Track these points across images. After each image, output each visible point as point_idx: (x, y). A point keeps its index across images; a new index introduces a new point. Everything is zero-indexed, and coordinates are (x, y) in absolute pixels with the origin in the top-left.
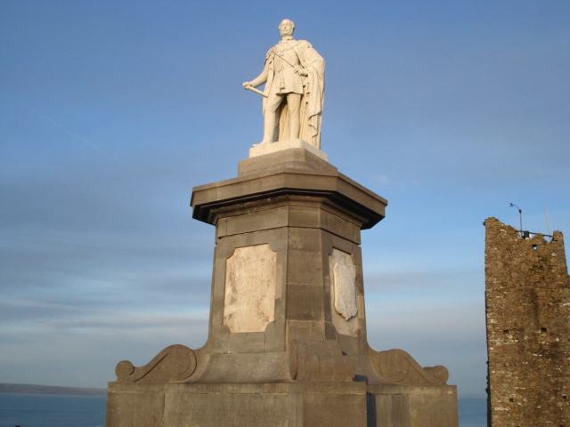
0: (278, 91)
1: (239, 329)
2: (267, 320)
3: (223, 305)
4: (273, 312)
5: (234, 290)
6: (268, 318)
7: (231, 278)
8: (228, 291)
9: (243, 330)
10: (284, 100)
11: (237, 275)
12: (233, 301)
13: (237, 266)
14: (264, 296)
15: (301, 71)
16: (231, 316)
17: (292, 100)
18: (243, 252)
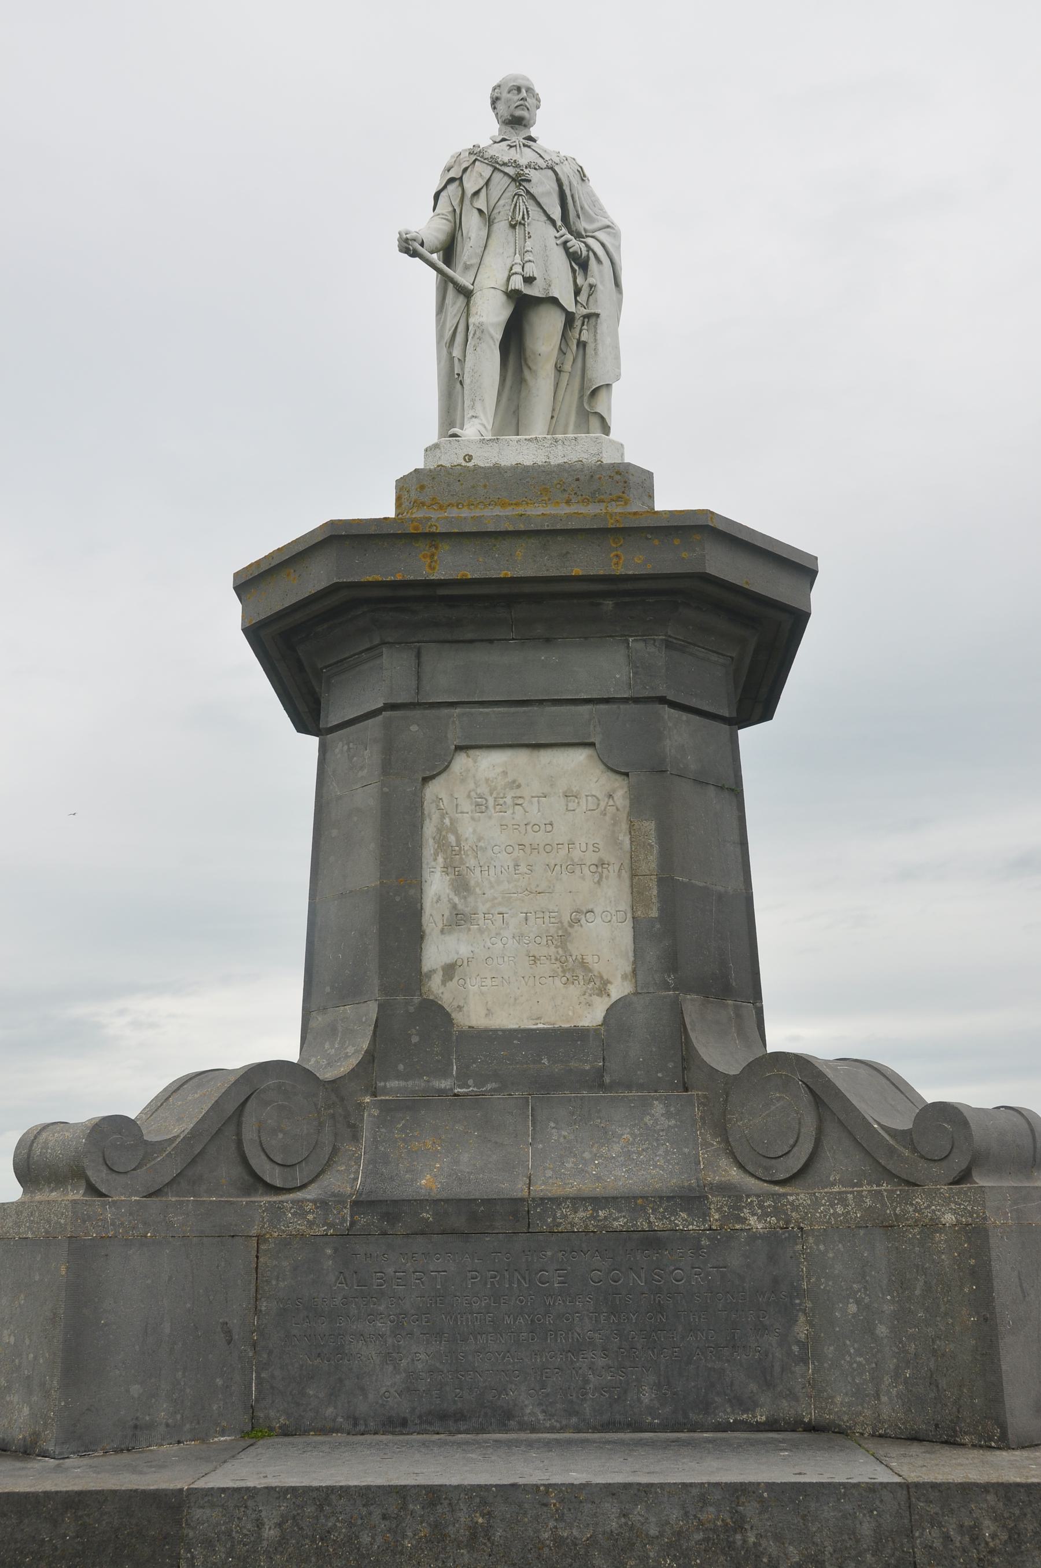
0: (517, 283)
1: (489, 1013)
2: (602, 990)
3: (417, 936)
4: (625, 966)
5: (461, 886)
6: (606, 983)
7: (442, 844)
8: (436, 885)
9: (509, 1019)
10: (522, 306)
11: (467, 830)
12: (458, 920)
13: (466, 806)
14: (579, 915)
15: (575, 245)
16: (450, 970)
17: (545, 333)
18: (489, 765)
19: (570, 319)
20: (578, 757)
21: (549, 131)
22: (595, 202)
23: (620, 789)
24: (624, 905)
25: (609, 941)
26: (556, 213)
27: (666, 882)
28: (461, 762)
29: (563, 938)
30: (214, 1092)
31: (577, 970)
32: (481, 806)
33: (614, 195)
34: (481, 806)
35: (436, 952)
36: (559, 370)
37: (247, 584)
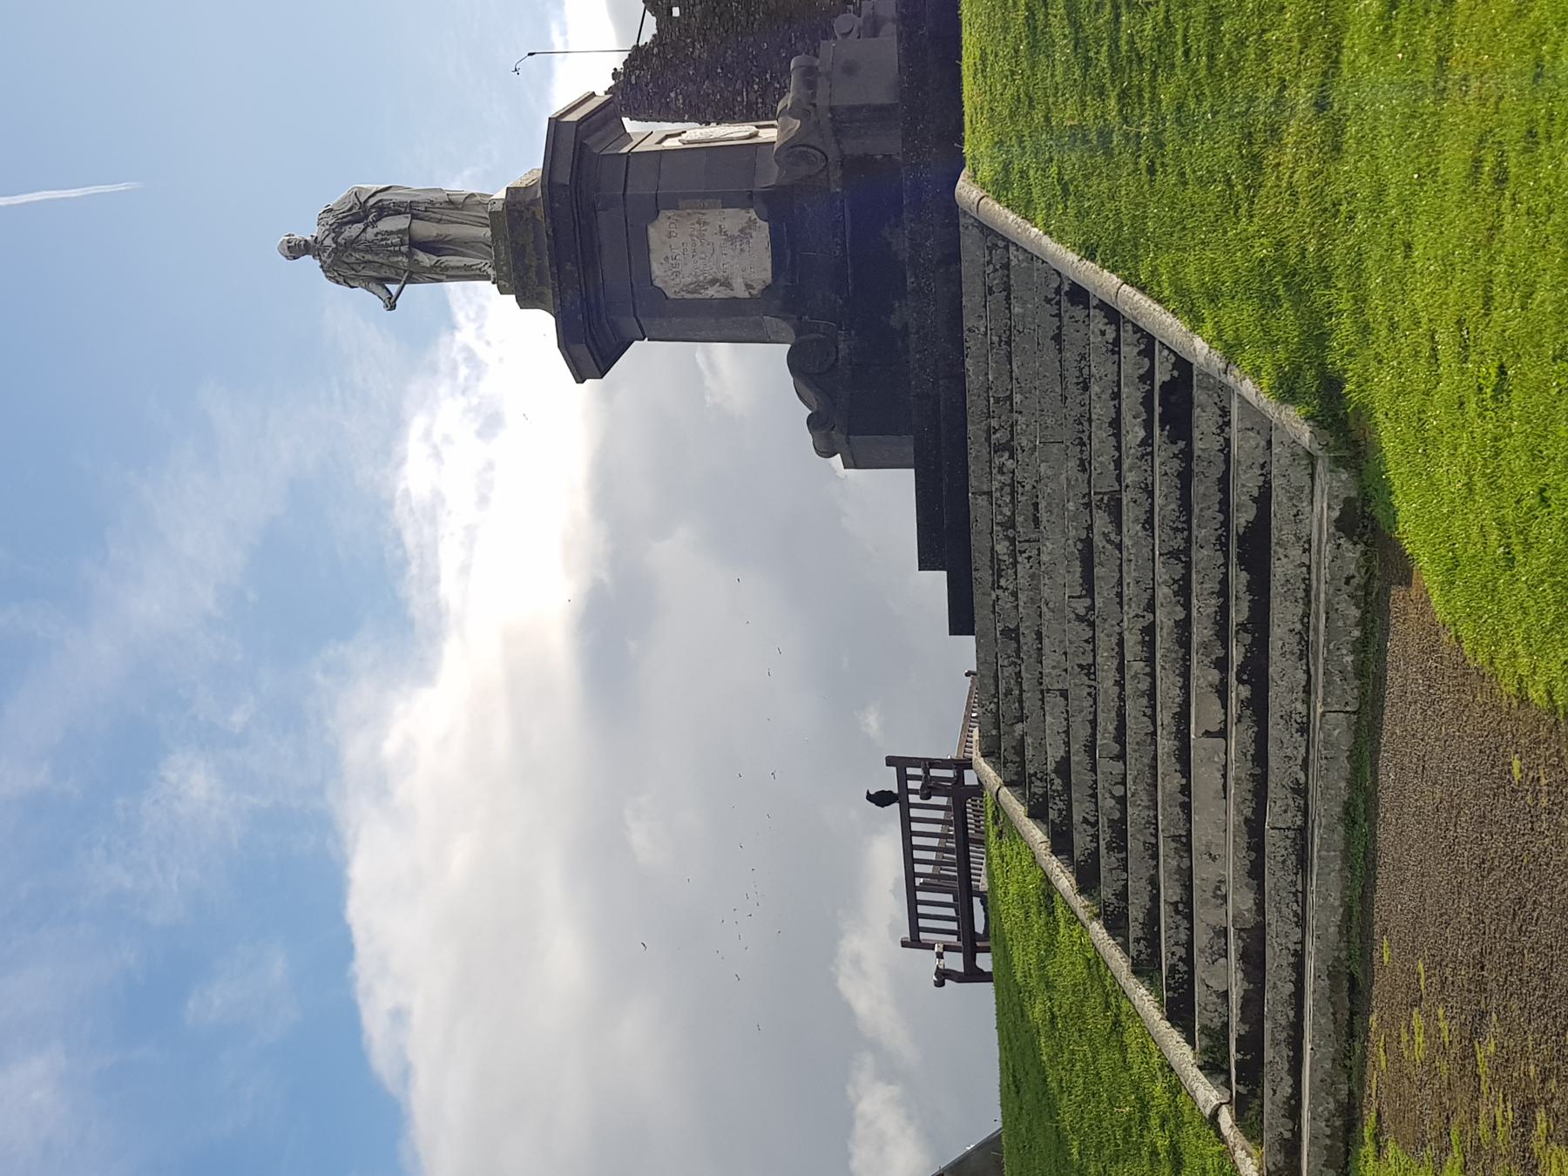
8: (712, 292)
12: (726, 284)
17: (425, 230)
18: (658, 270)
19: (414, 217)
20: (651, 230)
21: (309, 230)
22: (342, 202)
23: (664, 214)
24: (717, 212)
25: (733, 219)
26: (361, 226)
27: (706, 196)
28: (657, 283)
29: (731, 239)
30: (803, 387)
31: (744, 232)
32: (677, 274)
33: (337, 195)
34: (677, 274)
35: (741, 292)
36: (439, 221)
37: (580, 378)
